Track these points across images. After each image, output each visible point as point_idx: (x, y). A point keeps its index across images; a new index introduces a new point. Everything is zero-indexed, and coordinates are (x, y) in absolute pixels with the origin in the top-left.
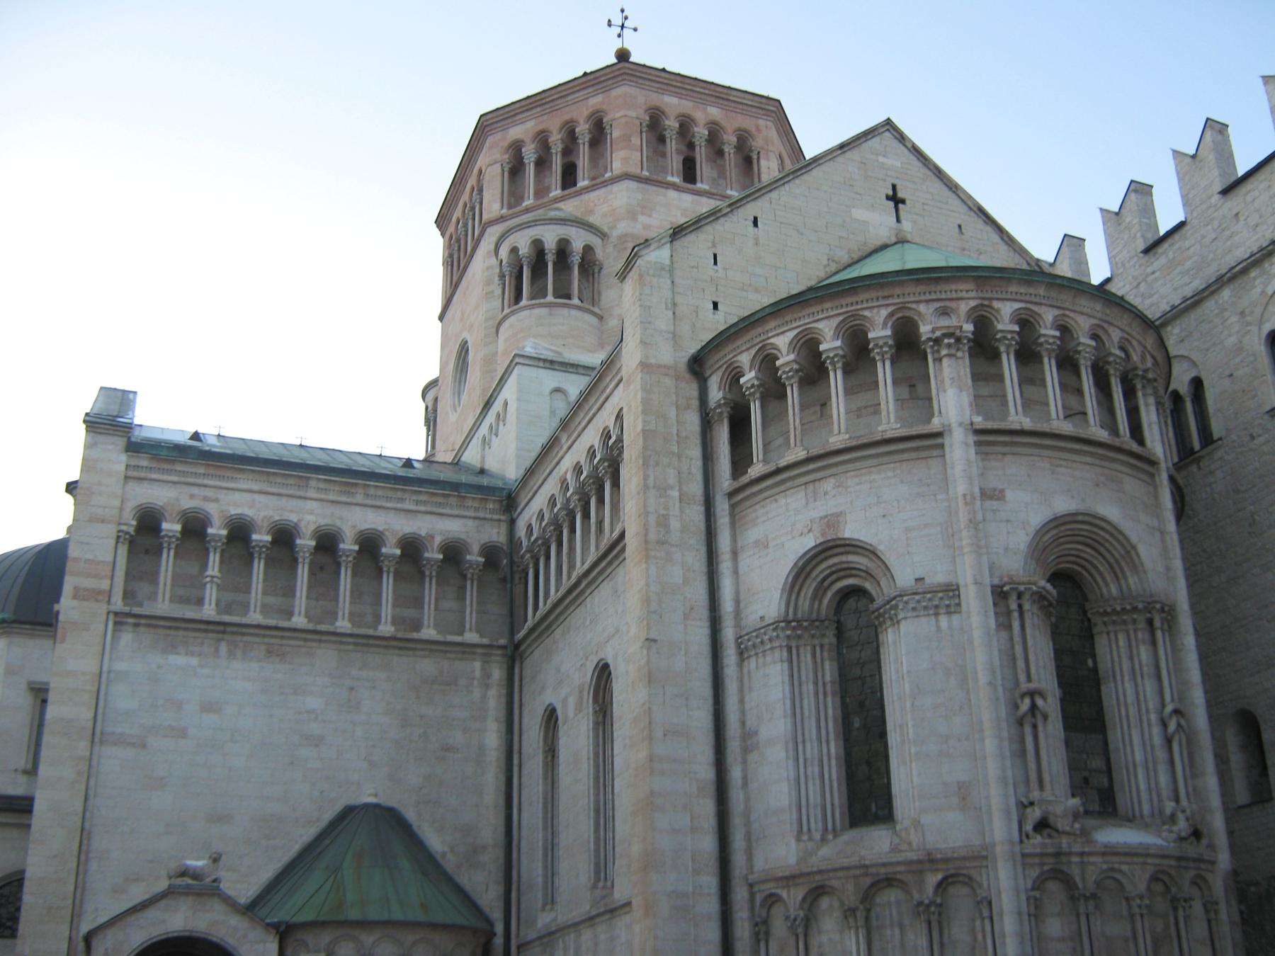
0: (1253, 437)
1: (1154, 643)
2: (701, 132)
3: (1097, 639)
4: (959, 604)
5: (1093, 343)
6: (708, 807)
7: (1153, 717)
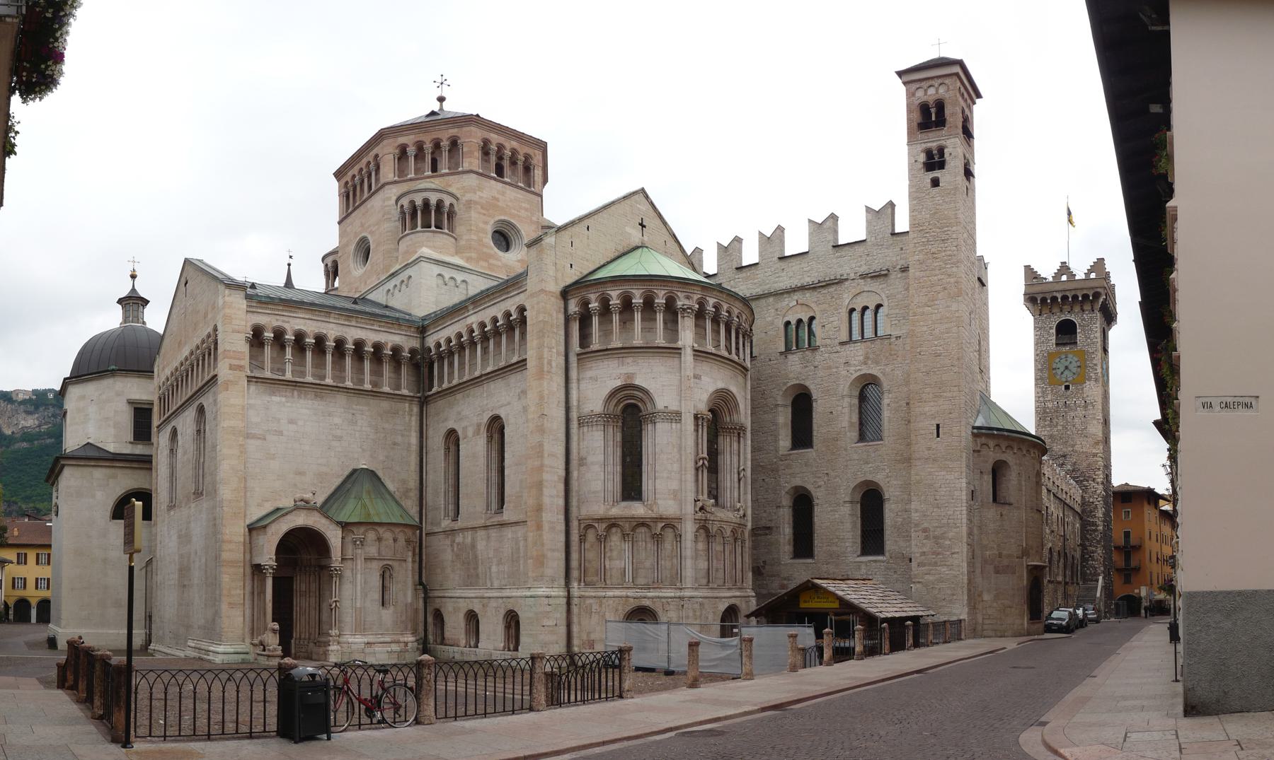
1: (739, 442)
3: (719, 437)
4: (680, 420)
5: (727, 314)
6: (561, 487)
7: (736, 471)
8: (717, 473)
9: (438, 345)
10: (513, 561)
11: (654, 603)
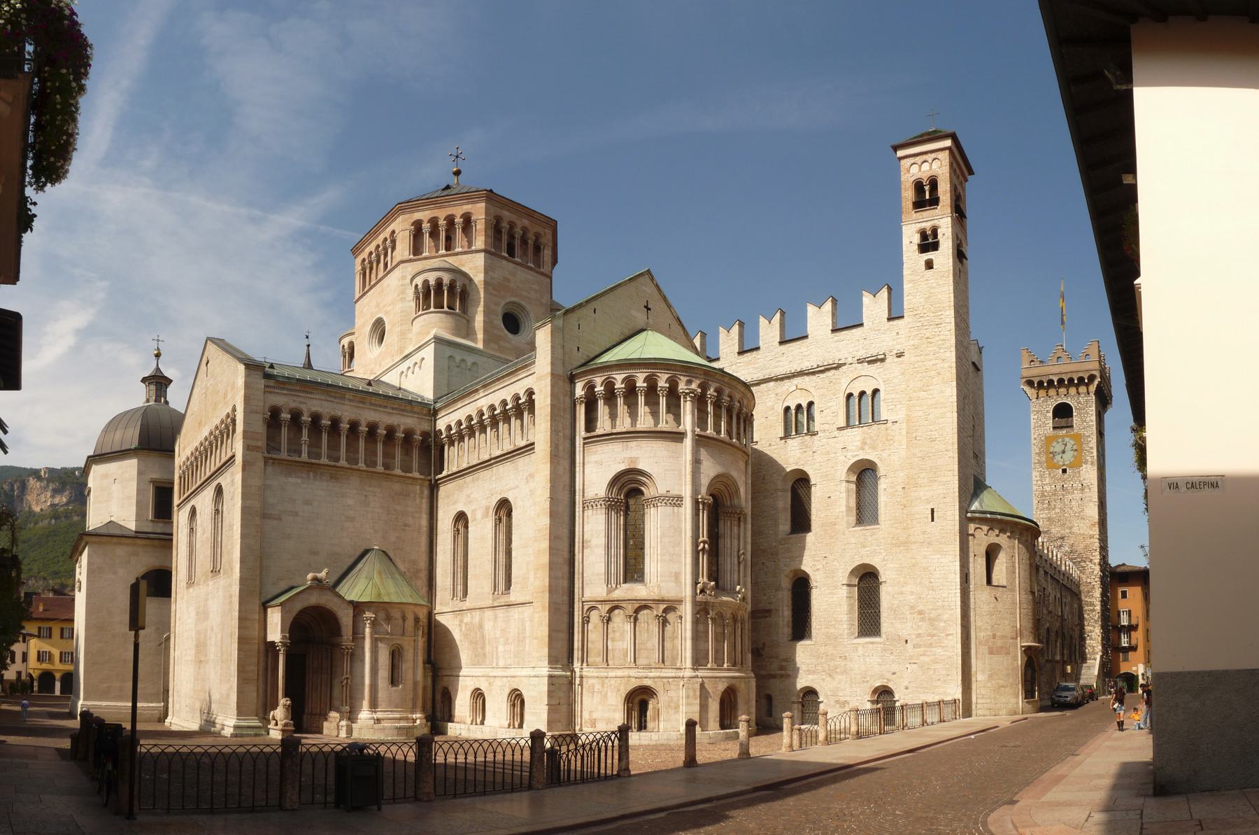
0: (770, 445)
1: (739, 526)
2: (518, 232)
5: (729, 399)
7: (736, 554)
8: (717, 555)
9: (449, 428)
10: (519, 641)
11: (655, 682)
